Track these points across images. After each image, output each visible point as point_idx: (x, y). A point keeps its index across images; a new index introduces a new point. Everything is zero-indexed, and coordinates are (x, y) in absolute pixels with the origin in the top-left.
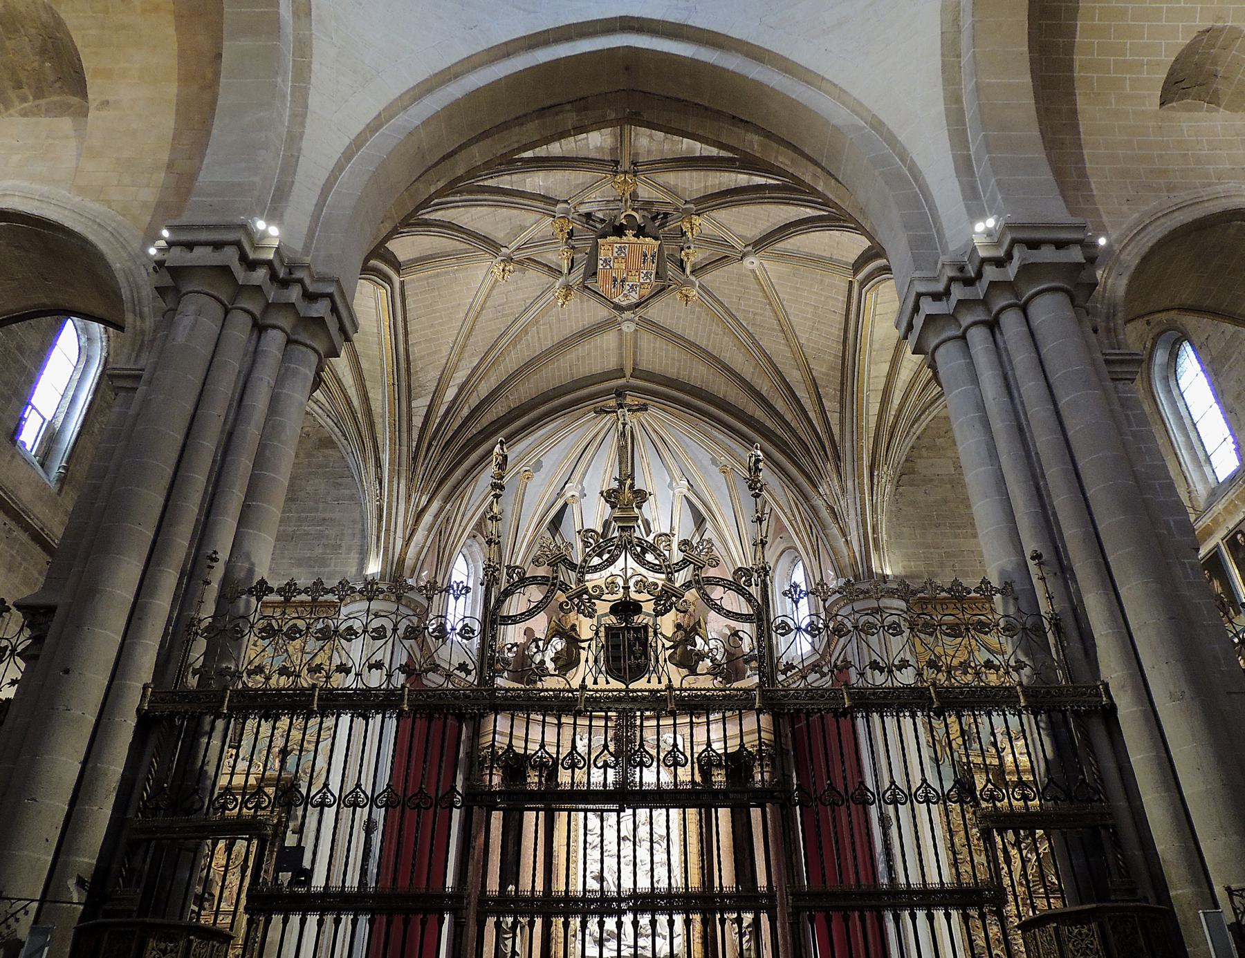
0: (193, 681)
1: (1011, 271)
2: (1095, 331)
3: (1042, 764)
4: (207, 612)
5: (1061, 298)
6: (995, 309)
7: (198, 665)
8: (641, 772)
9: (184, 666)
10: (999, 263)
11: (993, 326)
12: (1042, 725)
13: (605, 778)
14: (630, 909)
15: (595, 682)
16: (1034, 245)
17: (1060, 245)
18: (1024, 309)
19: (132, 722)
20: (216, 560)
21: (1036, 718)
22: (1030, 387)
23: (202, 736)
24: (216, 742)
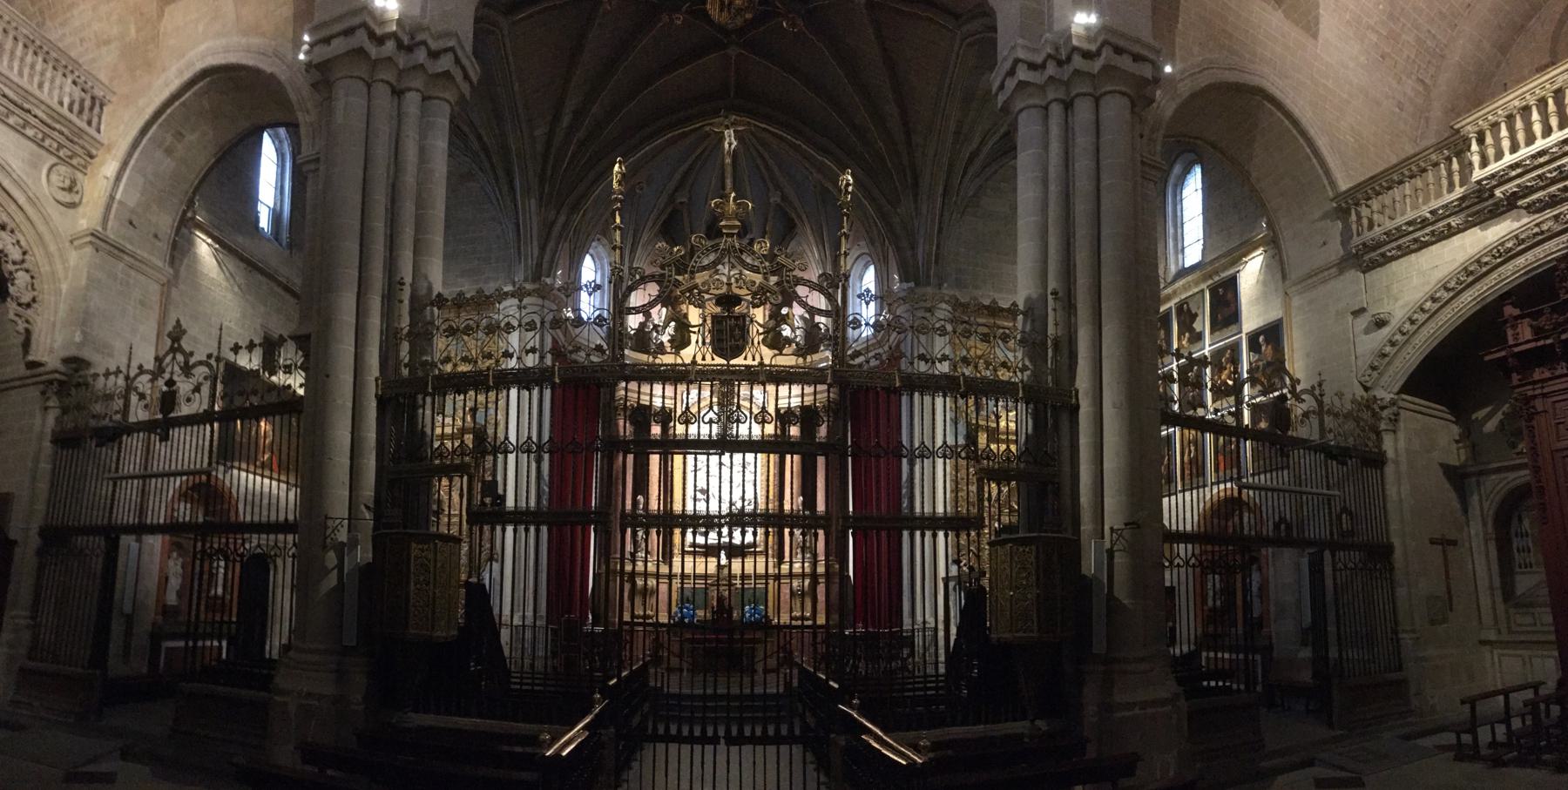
0: (405, 372)
6: (1074, 93)
8: (738, 427)
11: (1068, 105)
13: (711, 431)
14: (726, 523)
15: (704, 359)
17: (1137, 58)
18: (1097, 100)
19: (374, 404)
23: (418, 409)
24: (428, 412)
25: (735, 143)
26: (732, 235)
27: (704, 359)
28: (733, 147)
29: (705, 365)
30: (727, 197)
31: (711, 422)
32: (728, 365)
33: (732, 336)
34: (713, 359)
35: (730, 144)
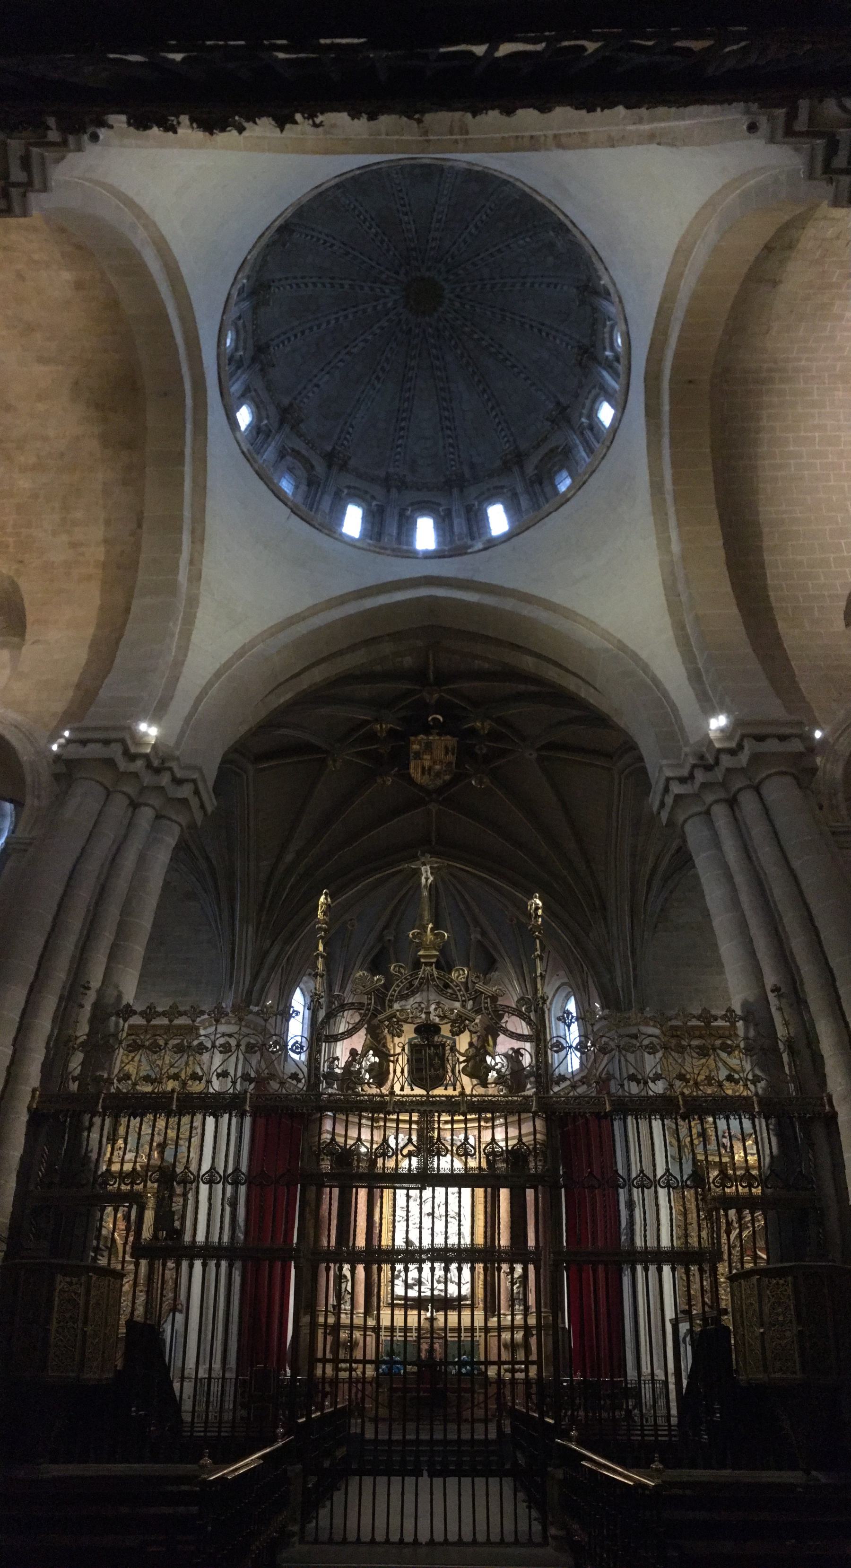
0: (74, 1087)
1: (744, 758)
2: (821, 807)
3: (768, 1159)
4: (83, 1030)
5: (788, 780)
6: (734, 790)
7: (78, 1071)
9: (65, 1075)
10: (732, 752)
11: (732, 803)
12: (771, 1127)
16: (760, 738)
17: (782, 738)
18: (757, 789)
19: (24, 1117)
20: (89, 988)
21: (767, 1122)
22: (766, 853)
23: (83, 1131)
24: (95, 1136)
25: (431, 879)
26: (431, 964)
27: (402, 1089)
28: (430, 881)
29: (403, 1096)
30: (424, 928)
31: (410, 1155)
32: (428, 1096)
33: (432, 1065)
34: (412, 1089)
35: (427, 879)
